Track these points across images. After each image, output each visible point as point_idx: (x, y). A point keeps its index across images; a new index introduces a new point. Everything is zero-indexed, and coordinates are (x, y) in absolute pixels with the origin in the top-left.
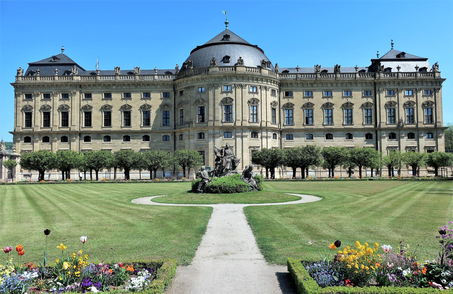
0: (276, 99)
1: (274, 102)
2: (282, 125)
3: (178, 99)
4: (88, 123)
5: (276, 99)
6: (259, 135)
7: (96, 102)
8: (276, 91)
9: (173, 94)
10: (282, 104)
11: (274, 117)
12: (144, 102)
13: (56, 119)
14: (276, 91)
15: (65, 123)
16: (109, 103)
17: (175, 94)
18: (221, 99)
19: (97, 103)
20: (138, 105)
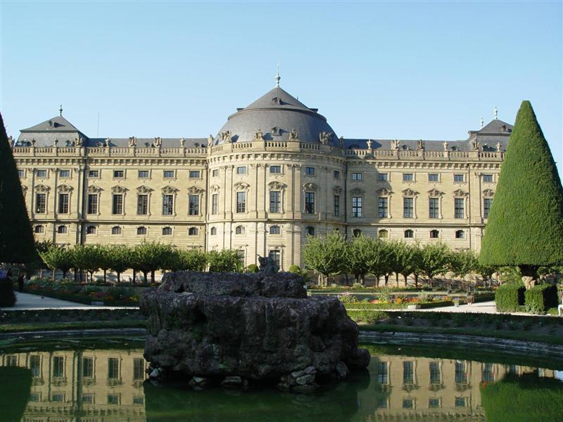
0: (341, 184)
1: (338, 187)
2: (347, 217)
3: (213, 181)
4: (92, 210)
5: (341, 184)
6: (316, 231)
7: (106, 182)
8: (341, 172)
9: (205, 172)
10: (347, 189)
11: (336, 206)
12: (166, 183)
13: (51, 202)
14: (341, 172)
15: (63, 208)
16: (121, 183)
17: (207, 173)
18: (267, 183)
19: (106, 184)
20: (158, 187)
